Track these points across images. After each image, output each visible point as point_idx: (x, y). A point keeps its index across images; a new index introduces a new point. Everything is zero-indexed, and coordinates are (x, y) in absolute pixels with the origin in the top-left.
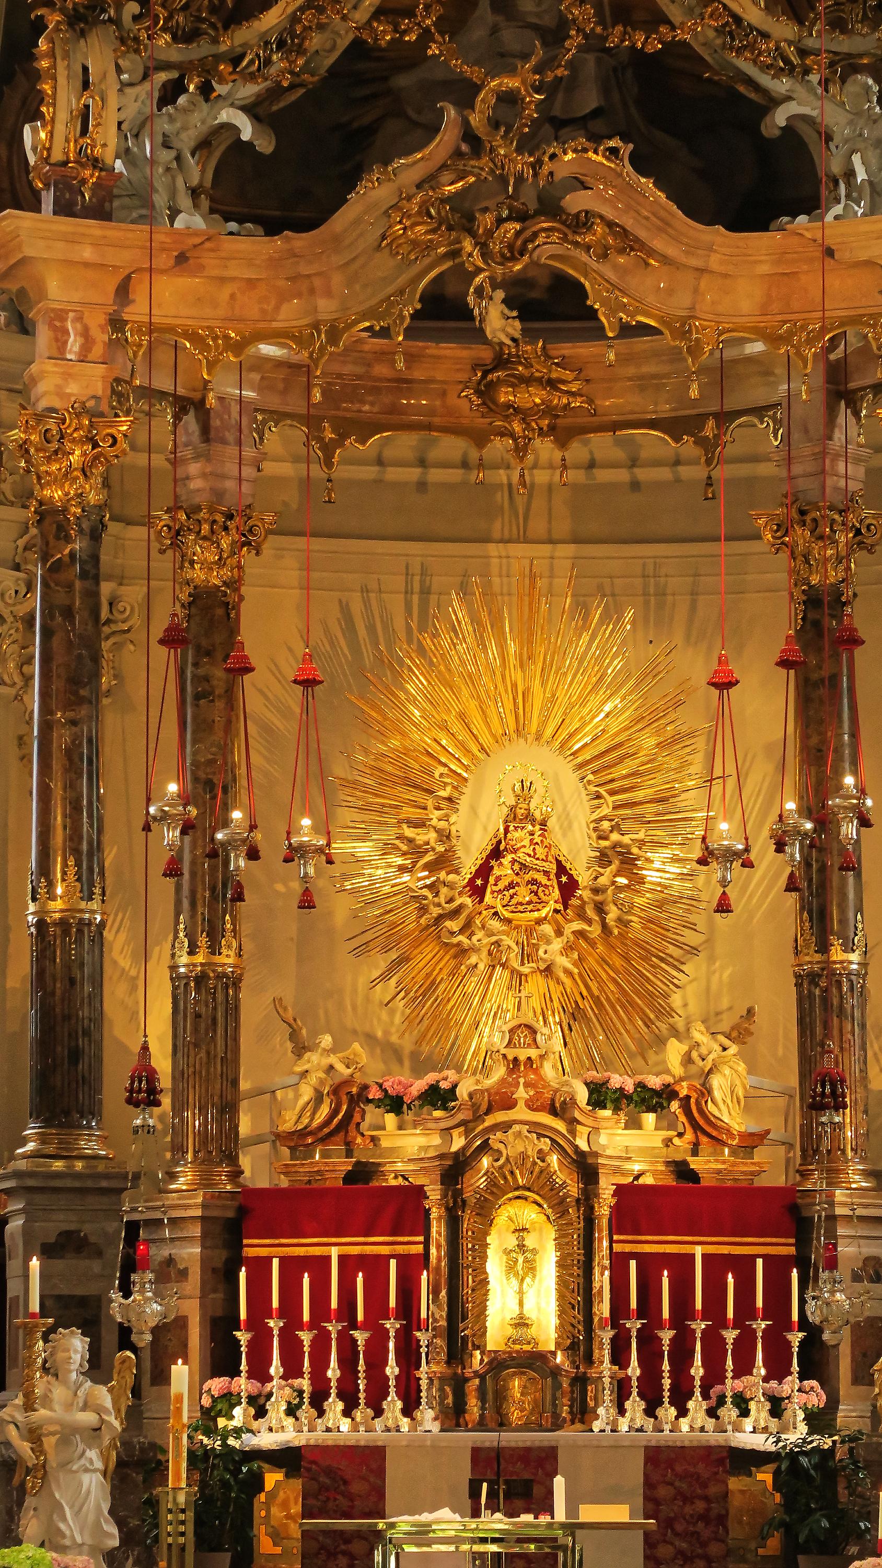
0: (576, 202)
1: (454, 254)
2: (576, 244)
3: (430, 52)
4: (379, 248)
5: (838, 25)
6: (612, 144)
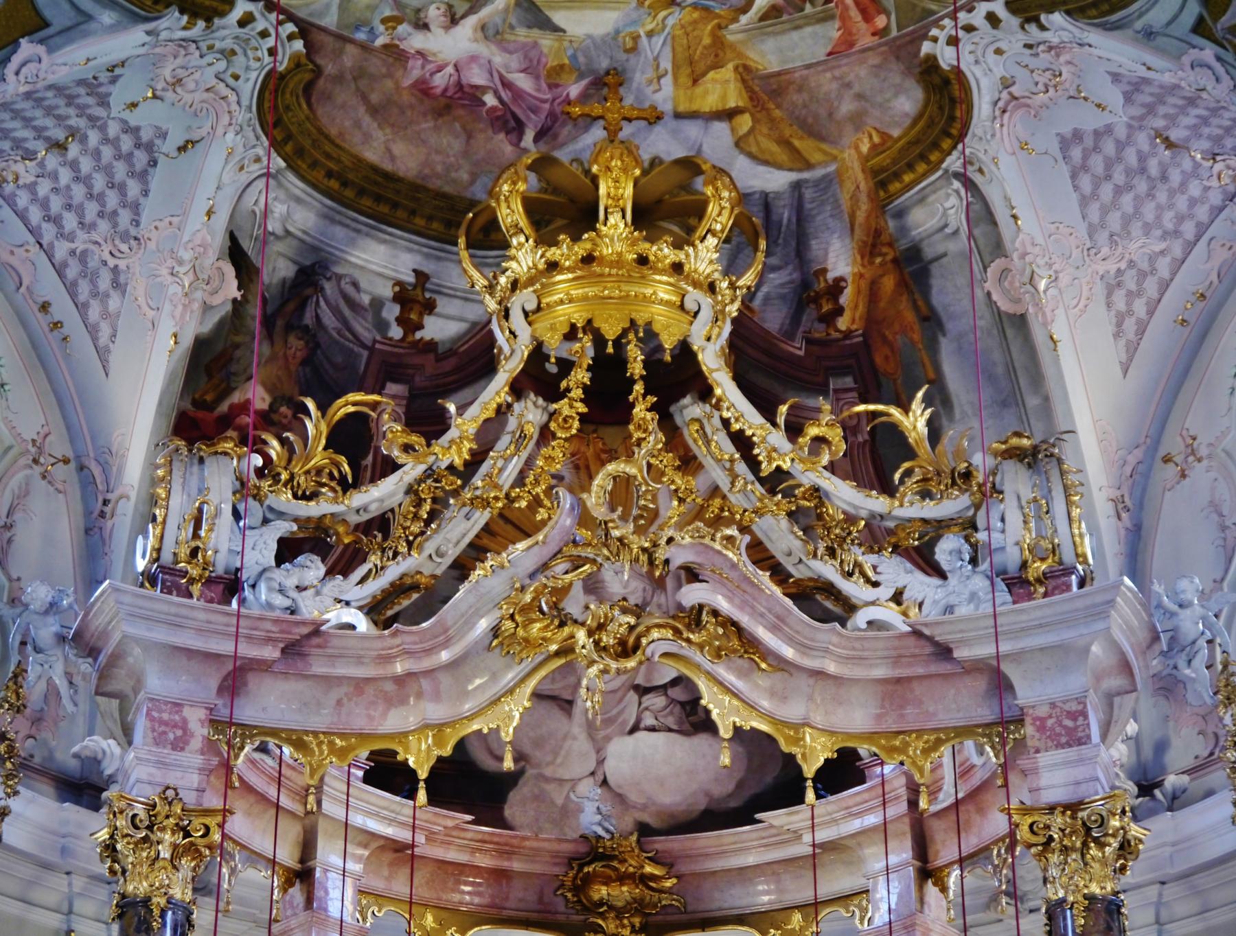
0: (692, 595)
1: (566, 650)
2: (688, 640)
3: (539, 518)
4: (489, 648)
6: (729, 532)
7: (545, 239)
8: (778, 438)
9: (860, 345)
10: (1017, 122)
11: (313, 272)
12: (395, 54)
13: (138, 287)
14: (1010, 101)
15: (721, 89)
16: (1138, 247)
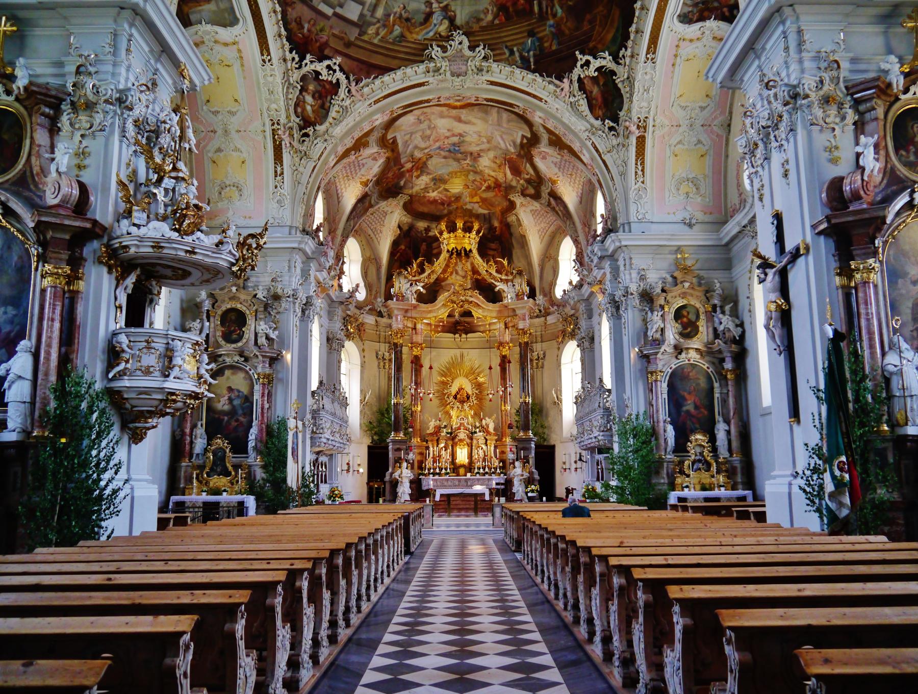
5: (507, 275)
7: (449, 232)
8: (485, 265)
9: (500, 241)
10: (523, 208)
11: (411, 227)
12: (424, 197)
13: (384, 232)
14: (522, 205)
15: (477, 199)
16: (543, 225)
